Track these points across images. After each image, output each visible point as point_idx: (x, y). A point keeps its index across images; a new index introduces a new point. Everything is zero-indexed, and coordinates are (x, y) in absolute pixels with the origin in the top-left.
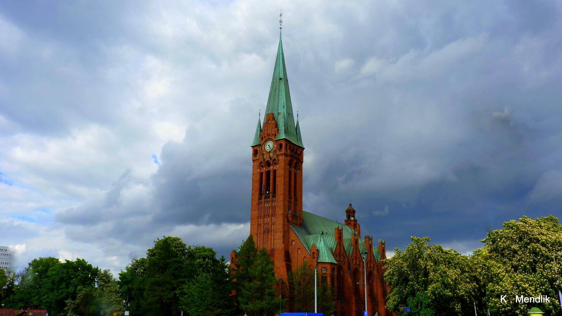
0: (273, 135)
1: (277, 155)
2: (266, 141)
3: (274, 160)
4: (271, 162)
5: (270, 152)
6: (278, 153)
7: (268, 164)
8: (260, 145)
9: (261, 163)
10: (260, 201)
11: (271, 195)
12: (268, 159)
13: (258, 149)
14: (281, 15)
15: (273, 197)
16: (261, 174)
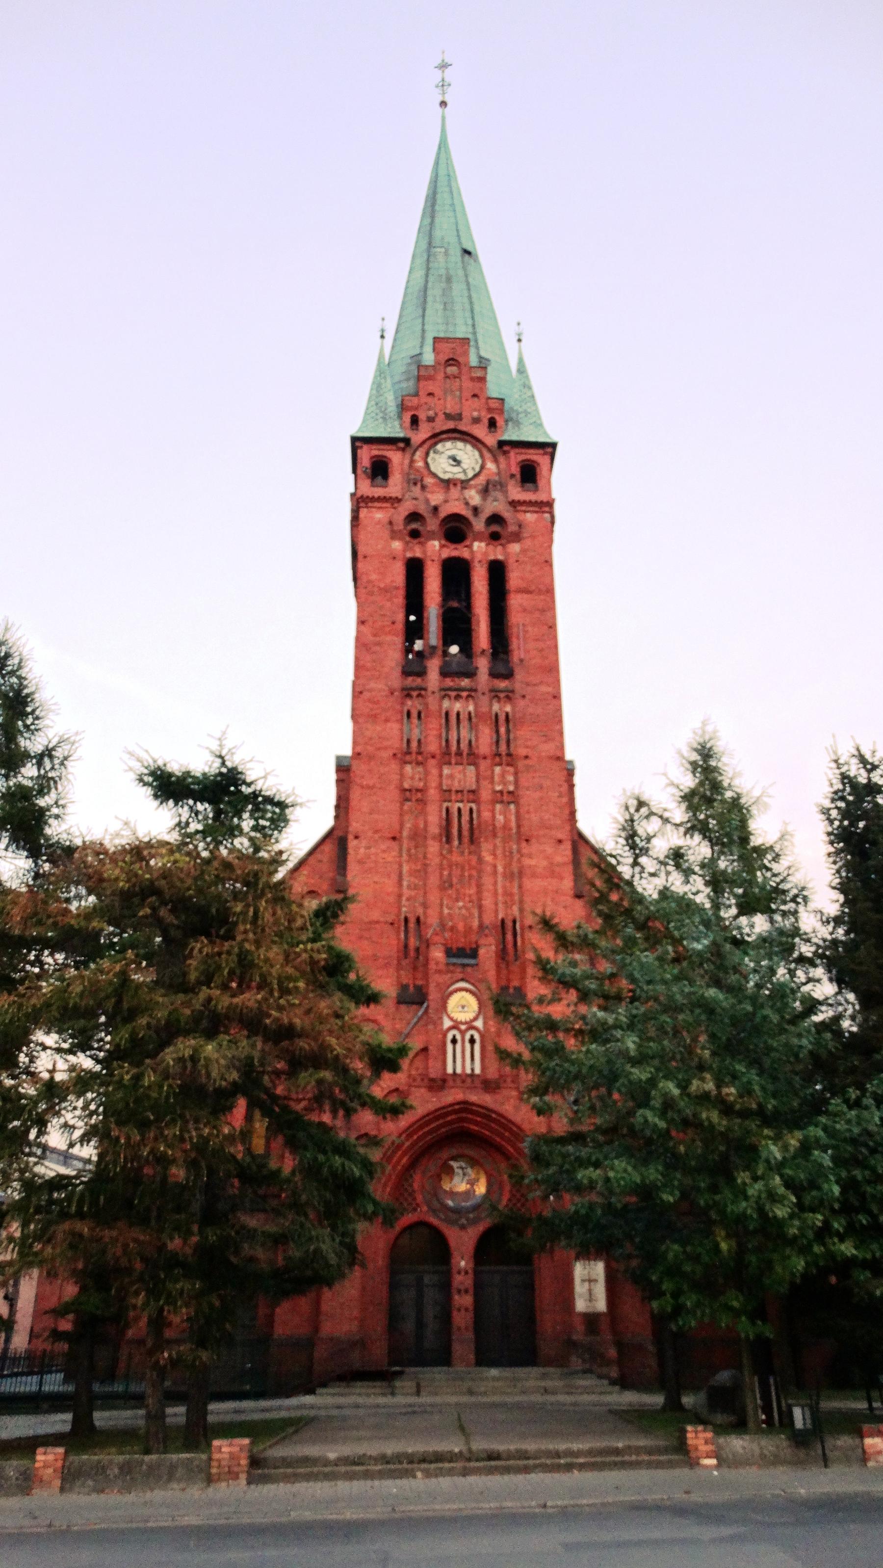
0: (476, 421)
1: (514, 504)
2: (436, 438)
3: (495, 519)
4: (479, 525)
5: (464, 484)
6: (516, 492)
7: (455, 529)
8: (407, 441)
9: (414, 517)
10: (410, 681)
11: (483, 664)
12: (455, 507)
13: (396, 458)
14: (443, 66)
15: (493, 675)
16: (415, 570)
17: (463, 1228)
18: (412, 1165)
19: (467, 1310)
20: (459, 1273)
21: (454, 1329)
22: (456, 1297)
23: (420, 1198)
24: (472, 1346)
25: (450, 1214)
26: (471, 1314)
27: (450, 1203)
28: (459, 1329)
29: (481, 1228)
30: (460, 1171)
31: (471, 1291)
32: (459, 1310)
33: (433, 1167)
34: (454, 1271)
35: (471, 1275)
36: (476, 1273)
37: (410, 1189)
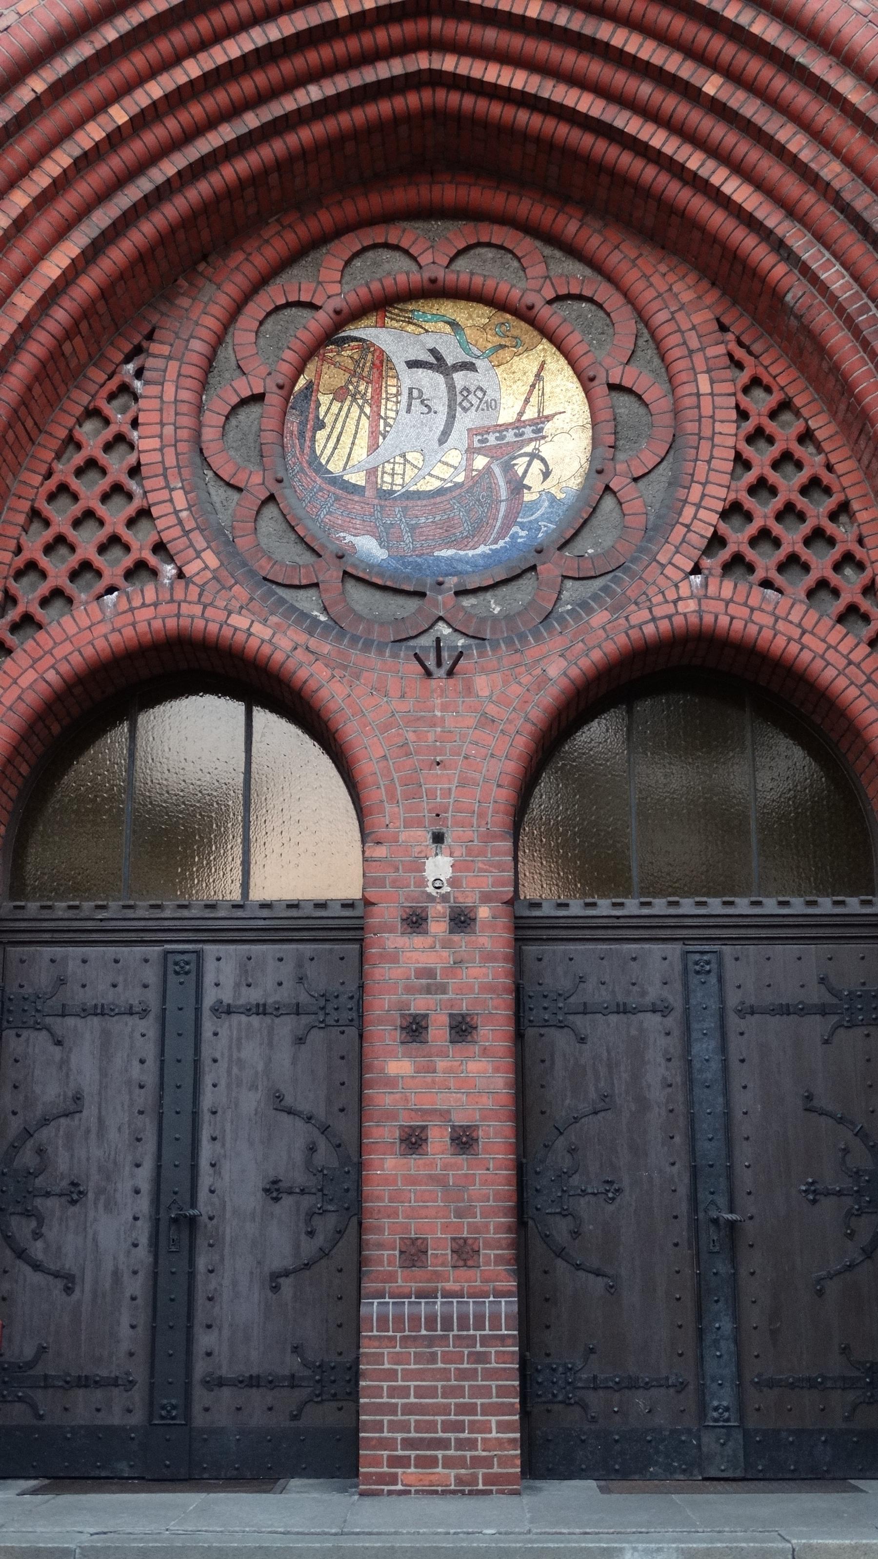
17: (442, 664)
18: (121, 314)
19: (464, 1141)
20: (415, 922)
21: (384, 1258)
22: (398, 1066)
23: (172, 505)
24: (503, 1357)
25: (359, 596)
26: (488, 1178)
27: (369, 547)
28: (414, 1253)
29: (558, 665)
30: (432, 383)
31: (494, 1033)
32: (413, 1141)
33: (258, 355)
34: (387, 913)
35: (491, 935)
36: (527, 929)
37: (117, 465)
